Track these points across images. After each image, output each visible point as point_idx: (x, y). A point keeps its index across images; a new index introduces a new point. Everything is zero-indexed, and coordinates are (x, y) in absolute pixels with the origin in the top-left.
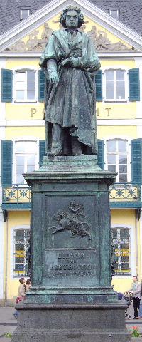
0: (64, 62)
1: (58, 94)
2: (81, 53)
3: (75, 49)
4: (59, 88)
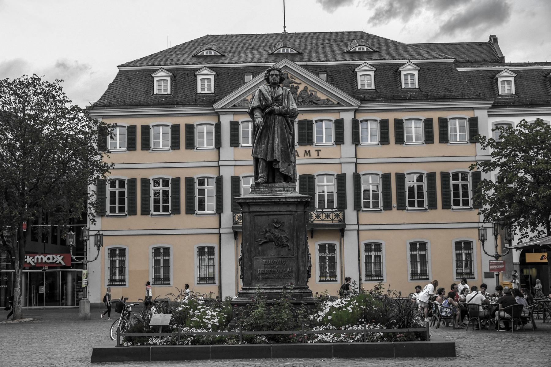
0: (267, 111)
1: (263, 135)
2: (282, 103)
3: (277, 100)
4: (264, 131)
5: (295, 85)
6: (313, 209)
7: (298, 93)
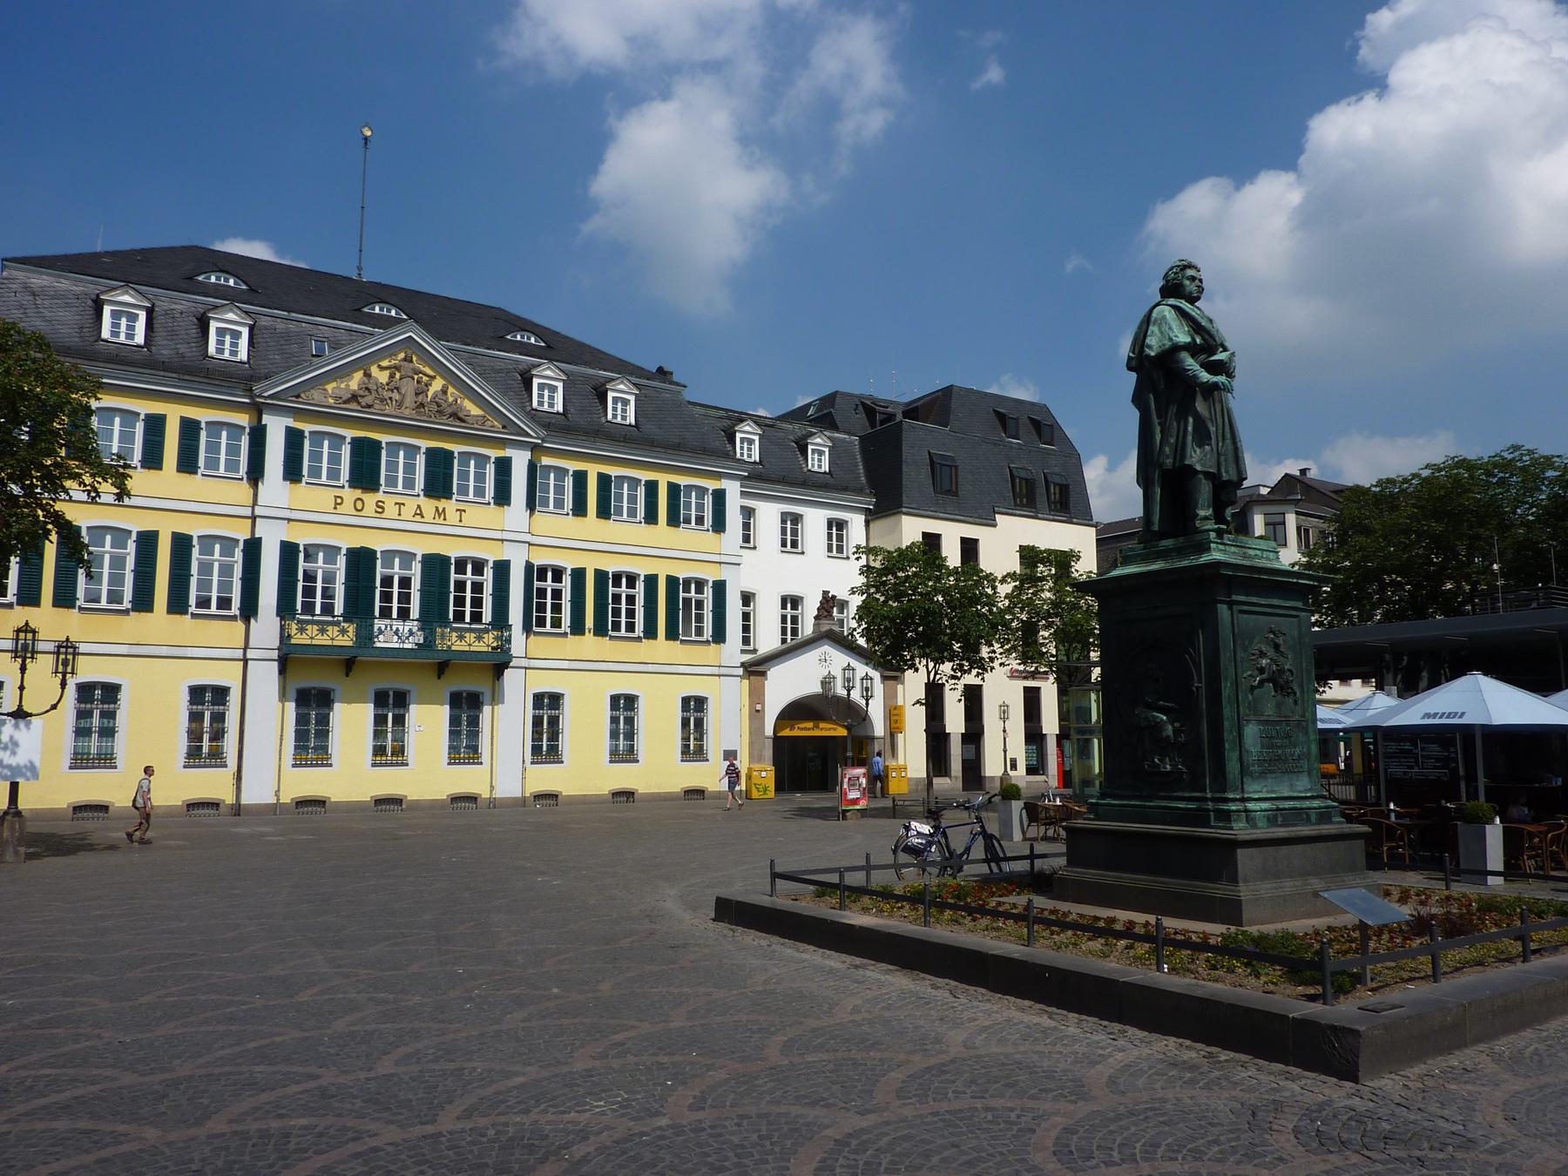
5: (425, 379)
6: (444, 622)
7: (430, 394)
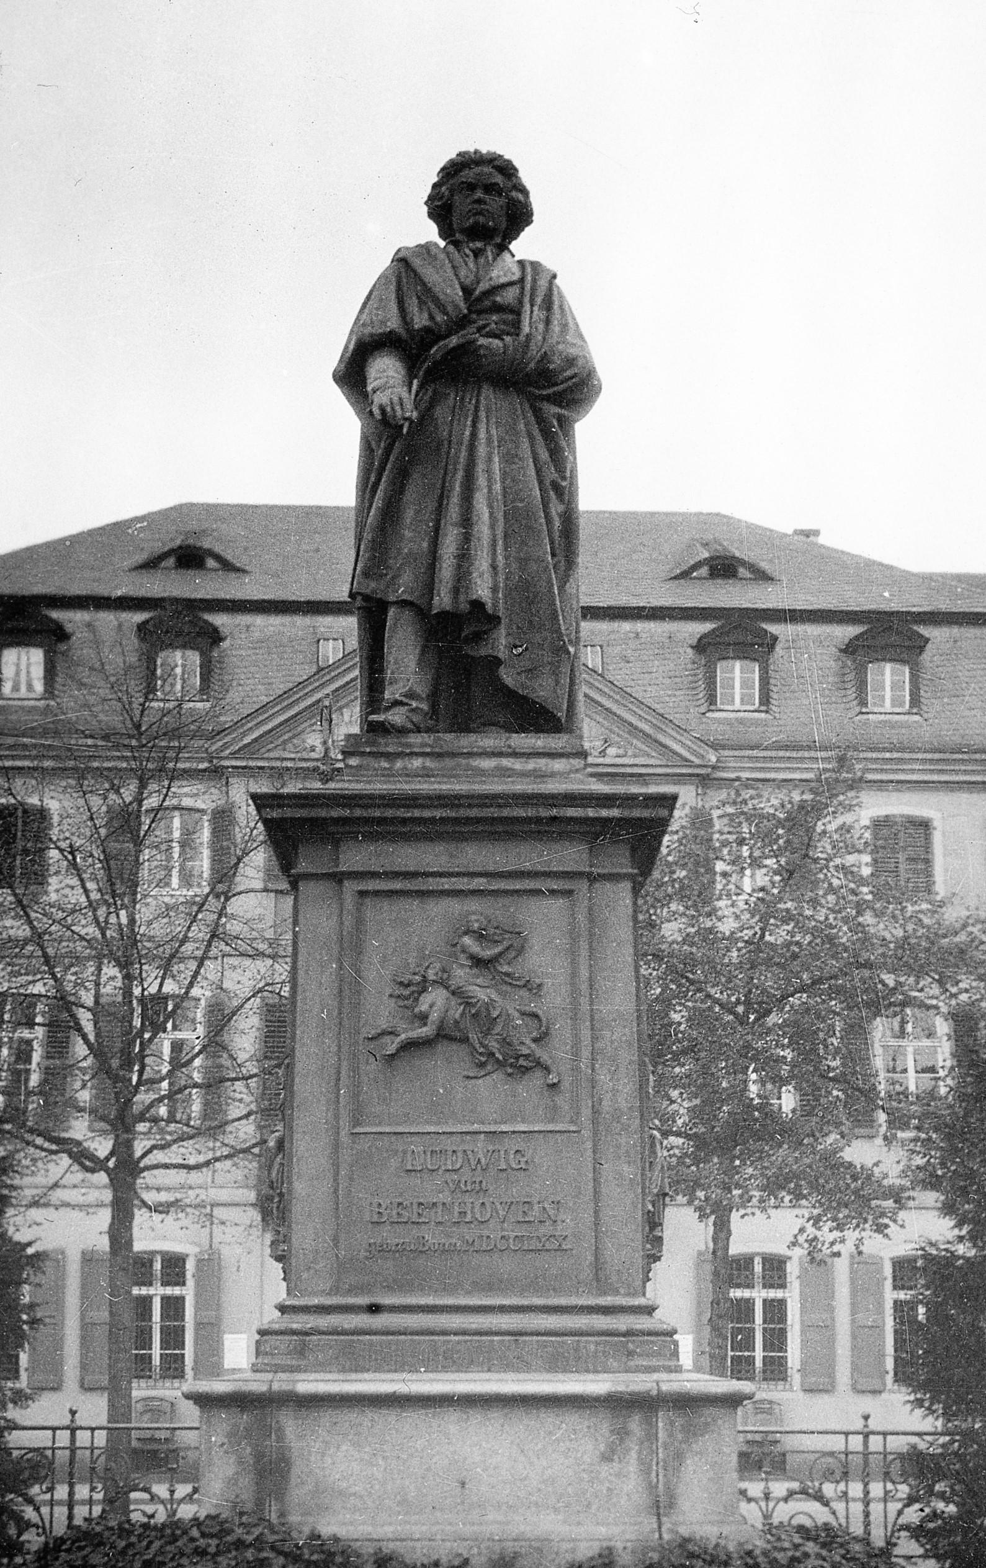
2: (517, 325)
